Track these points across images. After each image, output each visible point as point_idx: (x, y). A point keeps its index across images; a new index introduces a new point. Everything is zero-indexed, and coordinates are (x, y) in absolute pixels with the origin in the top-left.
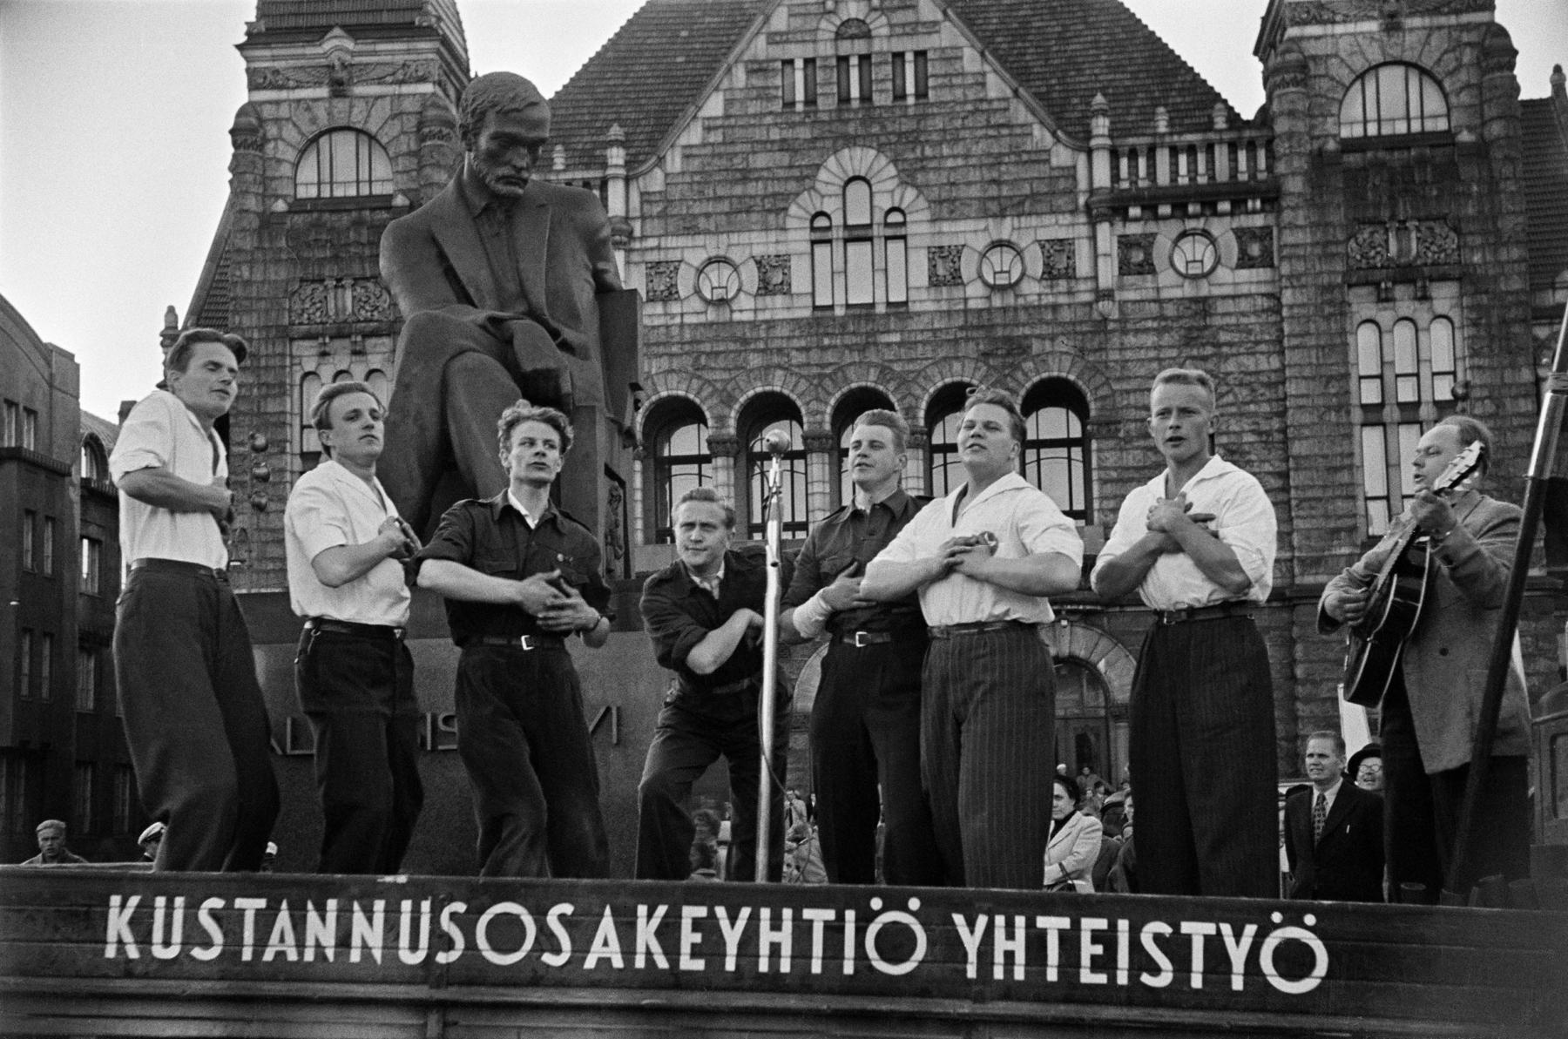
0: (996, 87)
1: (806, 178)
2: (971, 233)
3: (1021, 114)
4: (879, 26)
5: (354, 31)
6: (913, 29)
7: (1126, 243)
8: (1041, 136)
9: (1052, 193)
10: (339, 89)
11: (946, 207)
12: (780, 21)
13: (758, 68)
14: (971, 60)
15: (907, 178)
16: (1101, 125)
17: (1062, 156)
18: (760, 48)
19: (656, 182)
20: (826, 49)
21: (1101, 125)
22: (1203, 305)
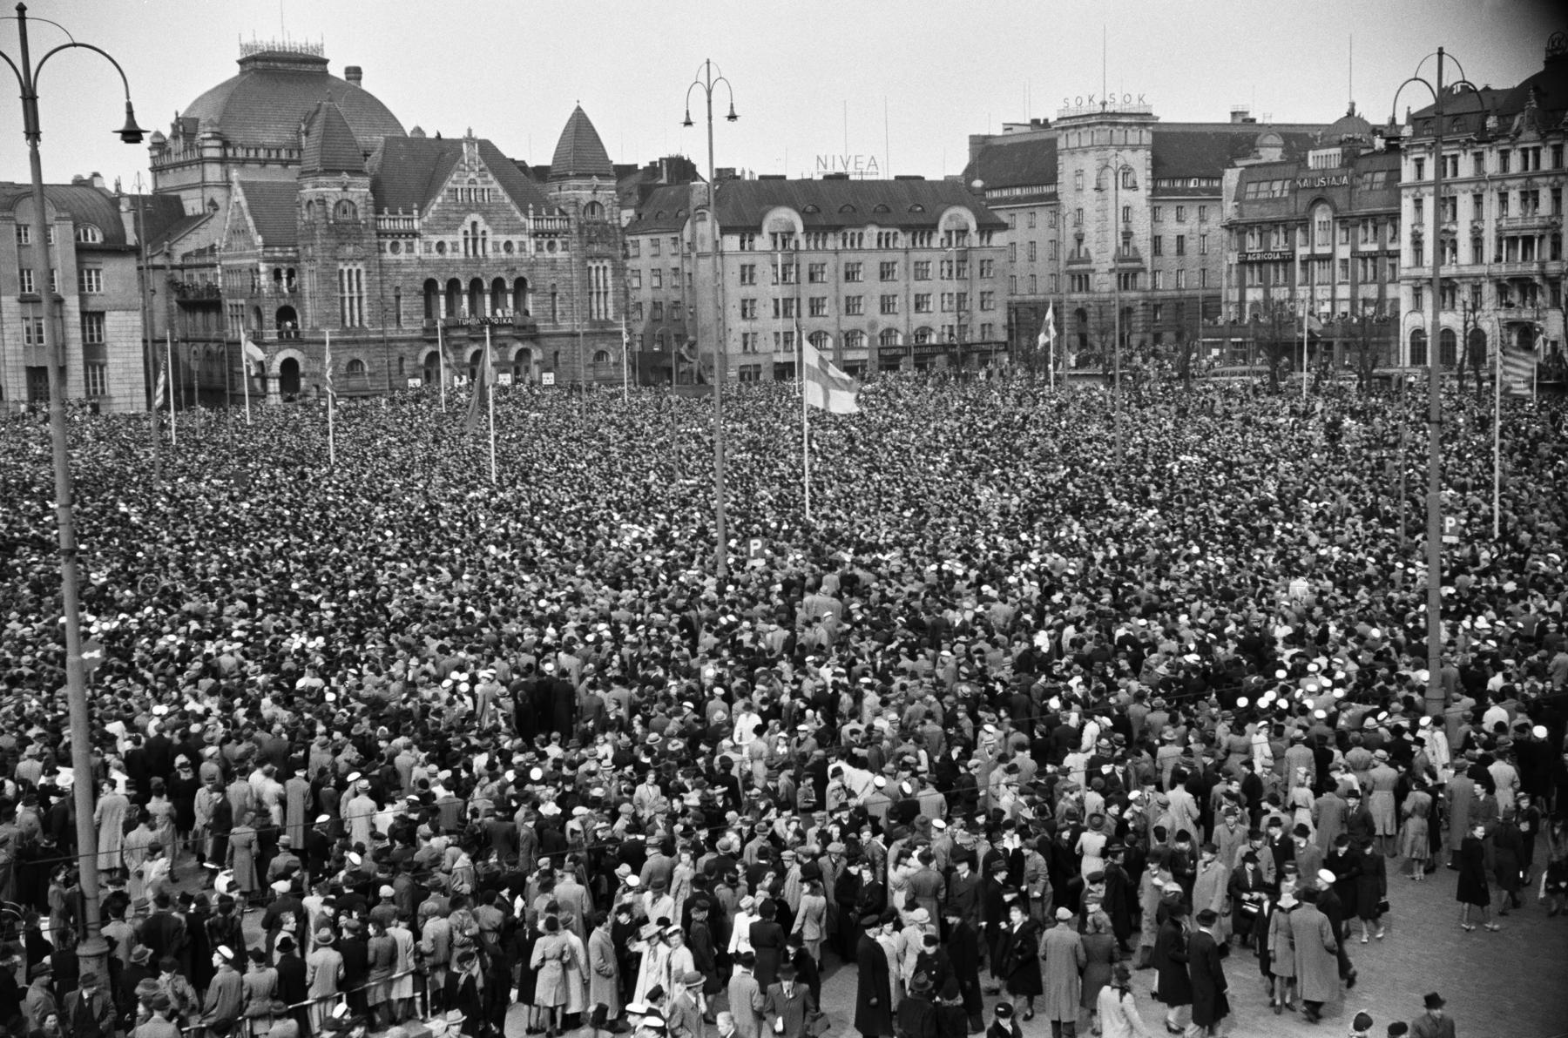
0: (507, 200)
1: (462, 220)
2: (503, 239)
3: (513, 207)
4: (479, 180)
5: (349, 172)
6: (487, 182)
7: (538, 244)
8: (518, 214)
9: (521, 229)
10: (345, 189)
11: (496, 231)
12: (455, 177)
13: (450, 191)
14: (501, 192)
15: (488, 222)
16: (531, 213)
17: (523, 219)
18: (450, 185)
19: (425, 220)
20: (466, 186)
21: (531, 213)
22: (554, 261)
